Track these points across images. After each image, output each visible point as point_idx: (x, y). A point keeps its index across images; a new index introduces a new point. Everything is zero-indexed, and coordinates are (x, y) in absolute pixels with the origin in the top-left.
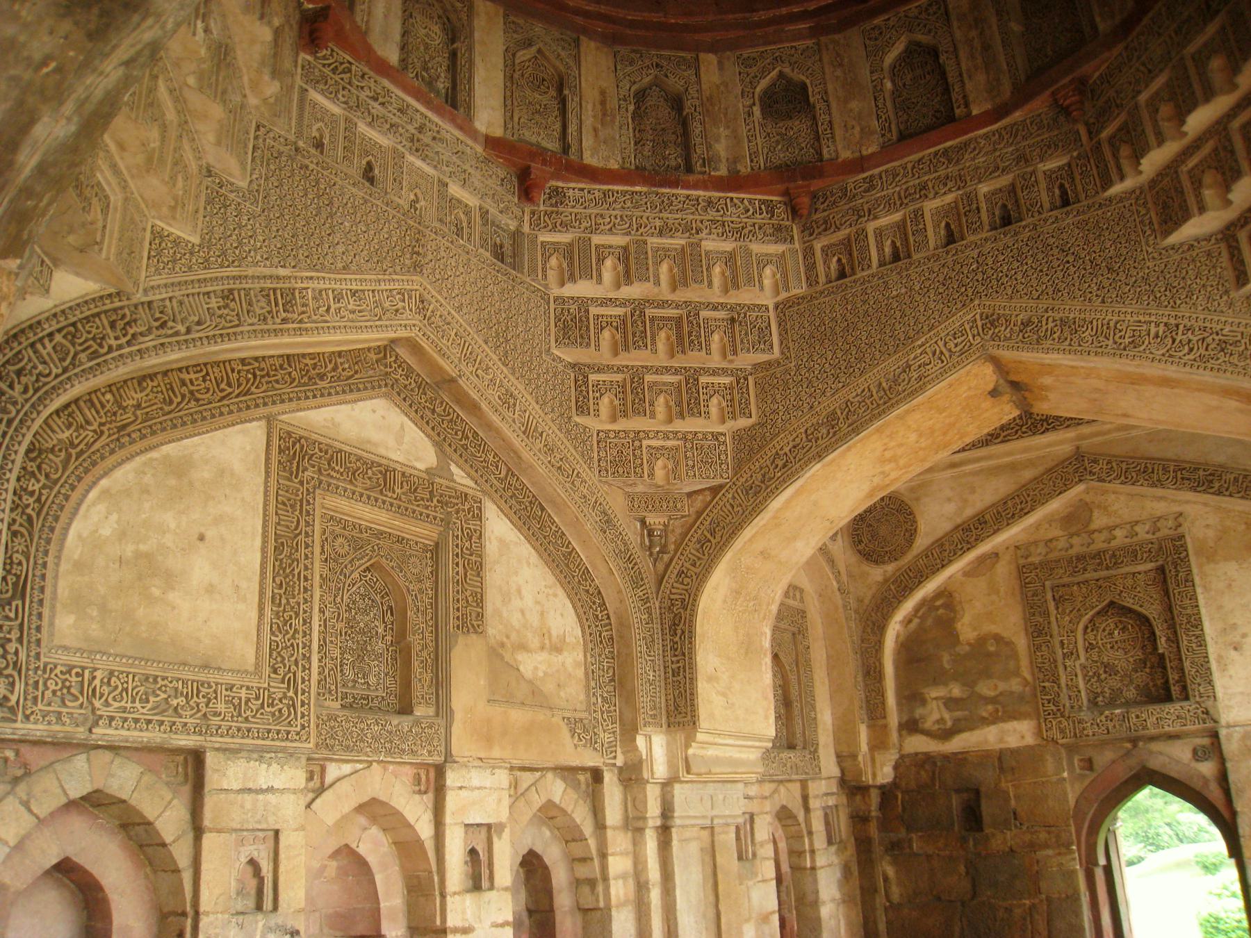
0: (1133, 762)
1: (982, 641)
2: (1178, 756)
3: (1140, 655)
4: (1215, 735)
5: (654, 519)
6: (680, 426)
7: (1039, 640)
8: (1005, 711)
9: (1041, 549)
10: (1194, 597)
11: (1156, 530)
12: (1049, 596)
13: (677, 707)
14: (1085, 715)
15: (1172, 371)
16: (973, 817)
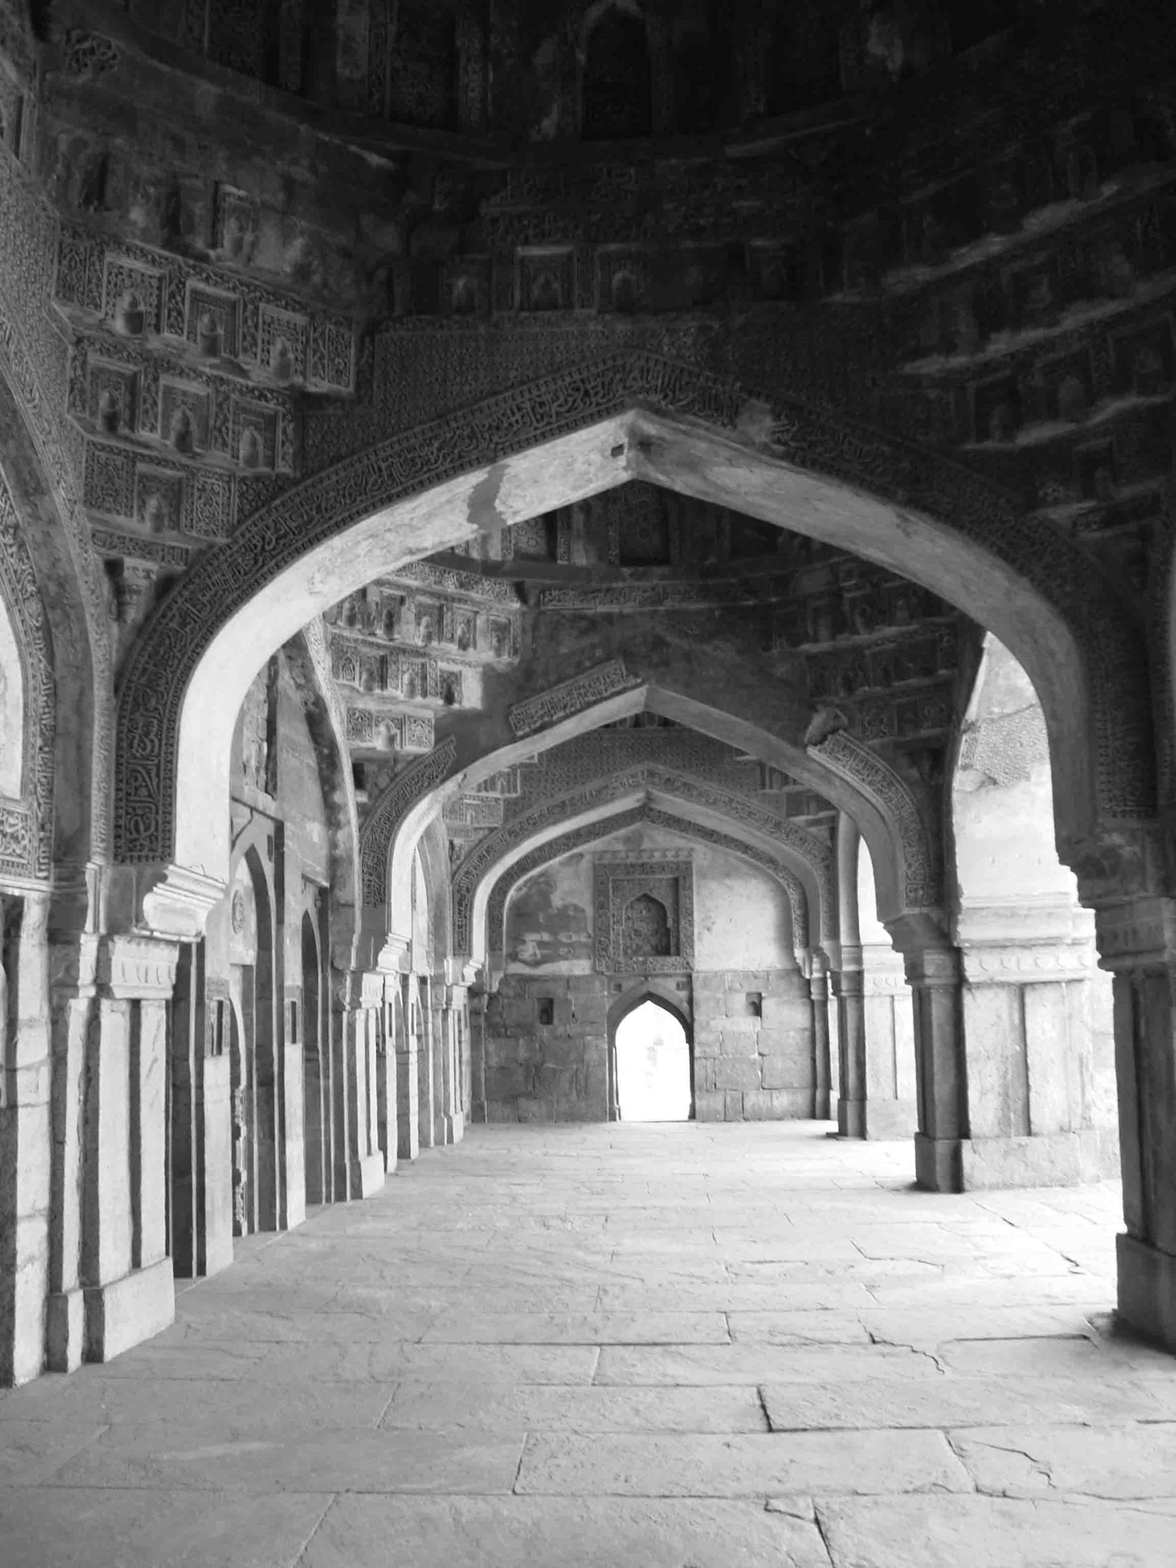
0: (644, 989)
1: (566, 908)
2: (668, 987)
3: (656, 926)
4: (690, 976)
5: (458, 841)
6: (483, 794)
7: (601, 912)
8: (572, 952)
9: (608, 856)
10: (691, 899)
11: (677, 855)
12: (610, 885)
13: (459, 945)
14: (621, 959)
15: (726, 818)
16: (547, 1012)
